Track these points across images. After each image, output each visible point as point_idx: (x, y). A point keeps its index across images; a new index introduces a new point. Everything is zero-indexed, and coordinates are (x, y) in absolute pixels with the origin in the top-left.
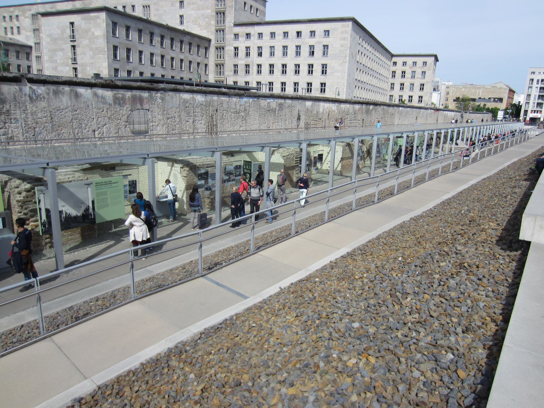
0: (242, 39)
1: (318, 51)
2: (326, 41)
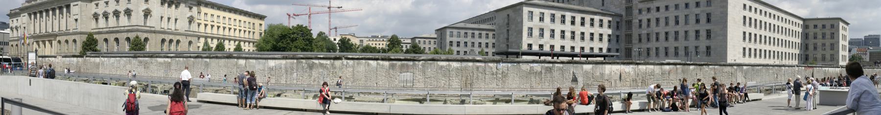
0: (653, 12)
1: (703, 19)
2: (708, 10)
